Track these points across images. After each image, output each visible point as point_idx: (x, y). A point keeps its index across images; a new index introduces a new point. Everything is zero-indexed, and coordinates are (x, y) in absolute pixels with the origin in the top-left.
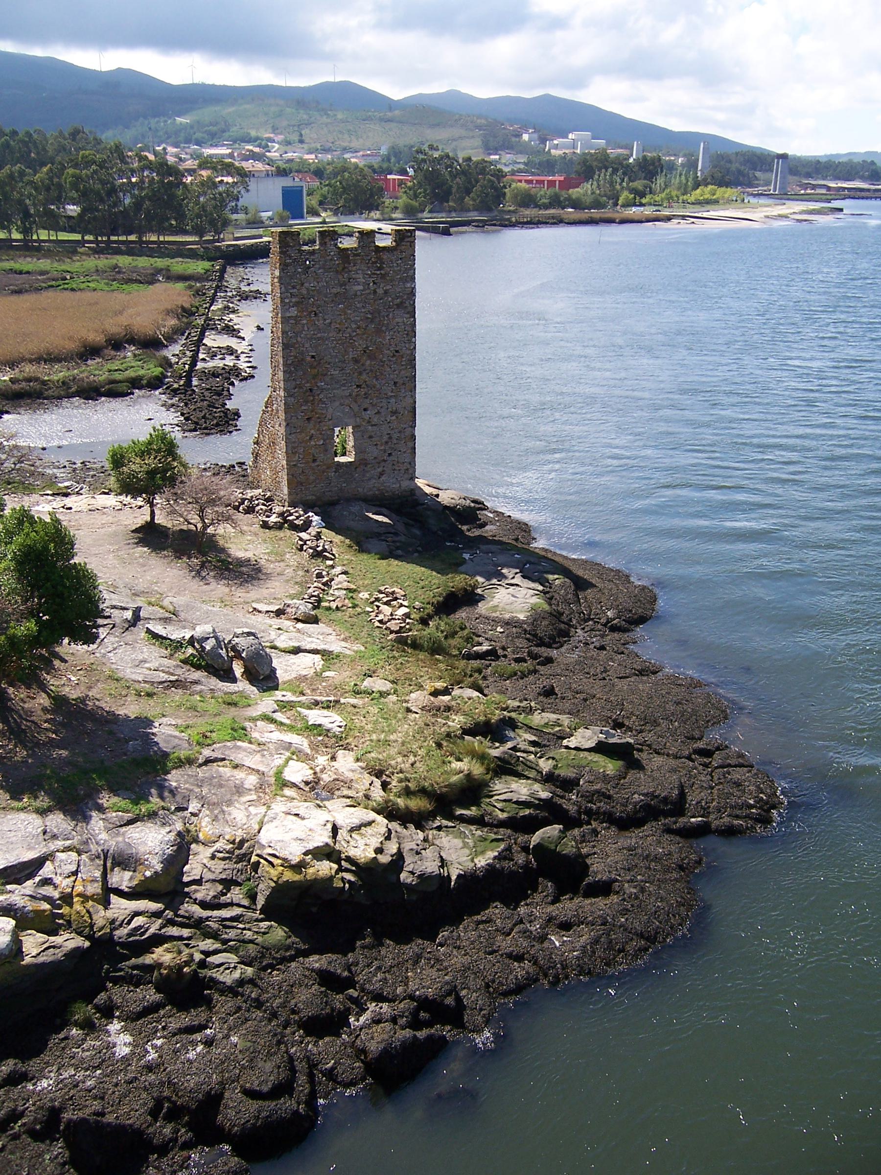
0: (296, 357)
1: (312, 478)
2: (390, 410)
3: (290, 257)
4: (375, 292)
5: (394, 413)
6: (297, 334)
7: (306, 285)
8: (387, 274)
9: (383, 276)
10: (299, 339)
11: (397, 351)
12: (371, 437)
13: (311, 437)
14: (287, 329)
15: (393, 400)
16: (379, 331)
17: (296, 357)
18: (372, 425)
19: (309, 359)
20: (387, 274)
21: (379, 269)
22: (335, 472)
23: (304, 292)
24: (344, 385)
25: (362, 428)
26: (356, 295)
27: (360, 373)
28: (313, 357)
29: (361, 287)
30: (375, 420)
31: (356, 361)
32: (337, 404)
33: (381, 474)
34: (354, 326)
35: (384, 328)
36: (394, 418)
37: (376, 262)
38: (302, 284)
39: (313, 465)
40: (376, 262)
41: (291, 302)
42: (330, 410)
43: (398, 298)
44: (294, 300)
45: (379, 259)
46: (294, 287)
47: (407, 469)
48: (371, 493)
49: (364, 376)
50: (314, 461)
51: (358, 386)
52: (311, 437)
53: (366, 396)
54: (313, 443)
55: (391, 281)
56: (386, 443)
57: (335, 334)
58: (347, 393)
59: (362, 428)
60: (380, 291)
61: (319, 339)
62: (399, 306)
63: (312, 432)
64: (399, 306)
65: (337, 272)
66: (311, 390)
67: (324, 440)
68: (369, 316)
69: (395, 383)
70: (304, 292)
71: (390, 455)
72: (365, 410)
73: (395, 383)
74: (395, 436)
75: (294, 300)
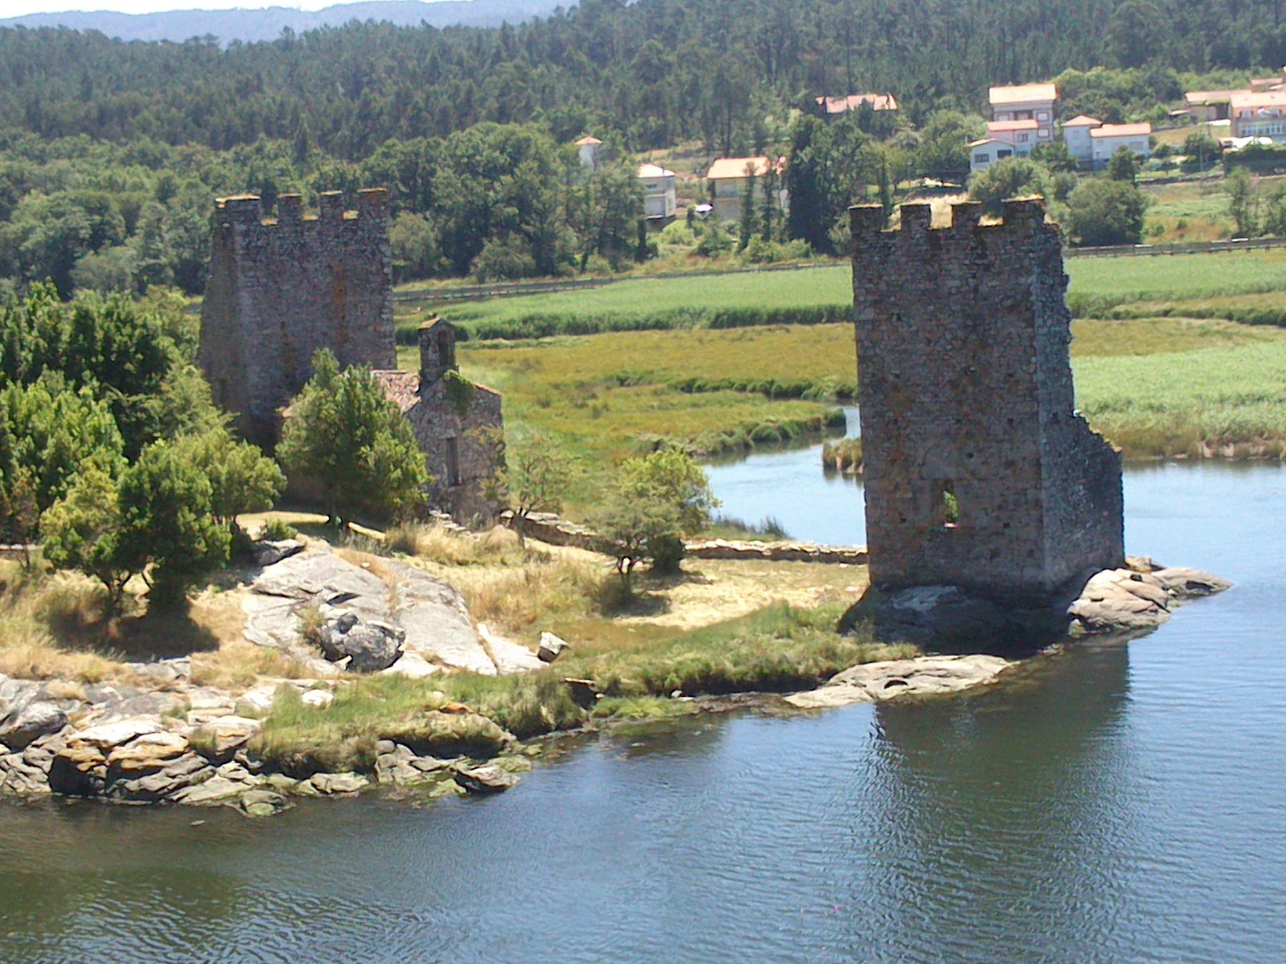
0: (873, 375)
1: (899, 545)
2: (1003, 459)
3: (865, 242)
4: (976, 290)
5: (1010, 464)
6: (875, 344)
7: (885, 278)
8: (992, 265)
9: (987, 268)
10: (878, 351)
11: (1011, 376)
12: (977, 497)
13: (897, 488)
14: (863, 336)
15: (1006, 446)
16: (984, 345)
17: (873, 375)
18: (980, 480)
19: (891, 378)
20: (992, 265)
21: (983, 256)
22: (930, 540)
23: (883, 286)
24: (937, 418)
25: (965, 482)
26: (950, 294)
27: (960, 403)
28: (898, 376)
29: (957, 283)
30: (983, 471)
31: (954, 384)
32: (930, 443)
33: (994, 554)
34: (948, 336)
35: (991, 341)
36: (1009, 472)
37: (975, 248)
38: (880, 277)
39: (904, 525)
40: (975, 248)
41: (865, 301)
42: (921, 452)
43: (1008, 298)
44: (870, 298)
45: (982, 243)
46: (870, 281)
47: (1032, 551)
48: (981, 579)
49: (965, 409)
50: (904, 520)
51: (958, 421)
52: (897, 488)
53: (969, 435)
54: (898, 495)
55: (999, 273)
56: (1000, 507)
57: (922, 346)
58: (941, 430)
59: (965, 482)
60: (984, 289)
61: (905, 351)
62: (1011, 309)
63: (899, 479)
64: (1011, 309)
65: (925, 262)
66: (896, 421)
67: (914, 493)
68: (970, 323)
69: (1011, 421)
70: (883, 286)
71: (1007, 525)
72: (971, 456)
73: (1011, 421)
74: (1011, 498)
75: (870, 298)
